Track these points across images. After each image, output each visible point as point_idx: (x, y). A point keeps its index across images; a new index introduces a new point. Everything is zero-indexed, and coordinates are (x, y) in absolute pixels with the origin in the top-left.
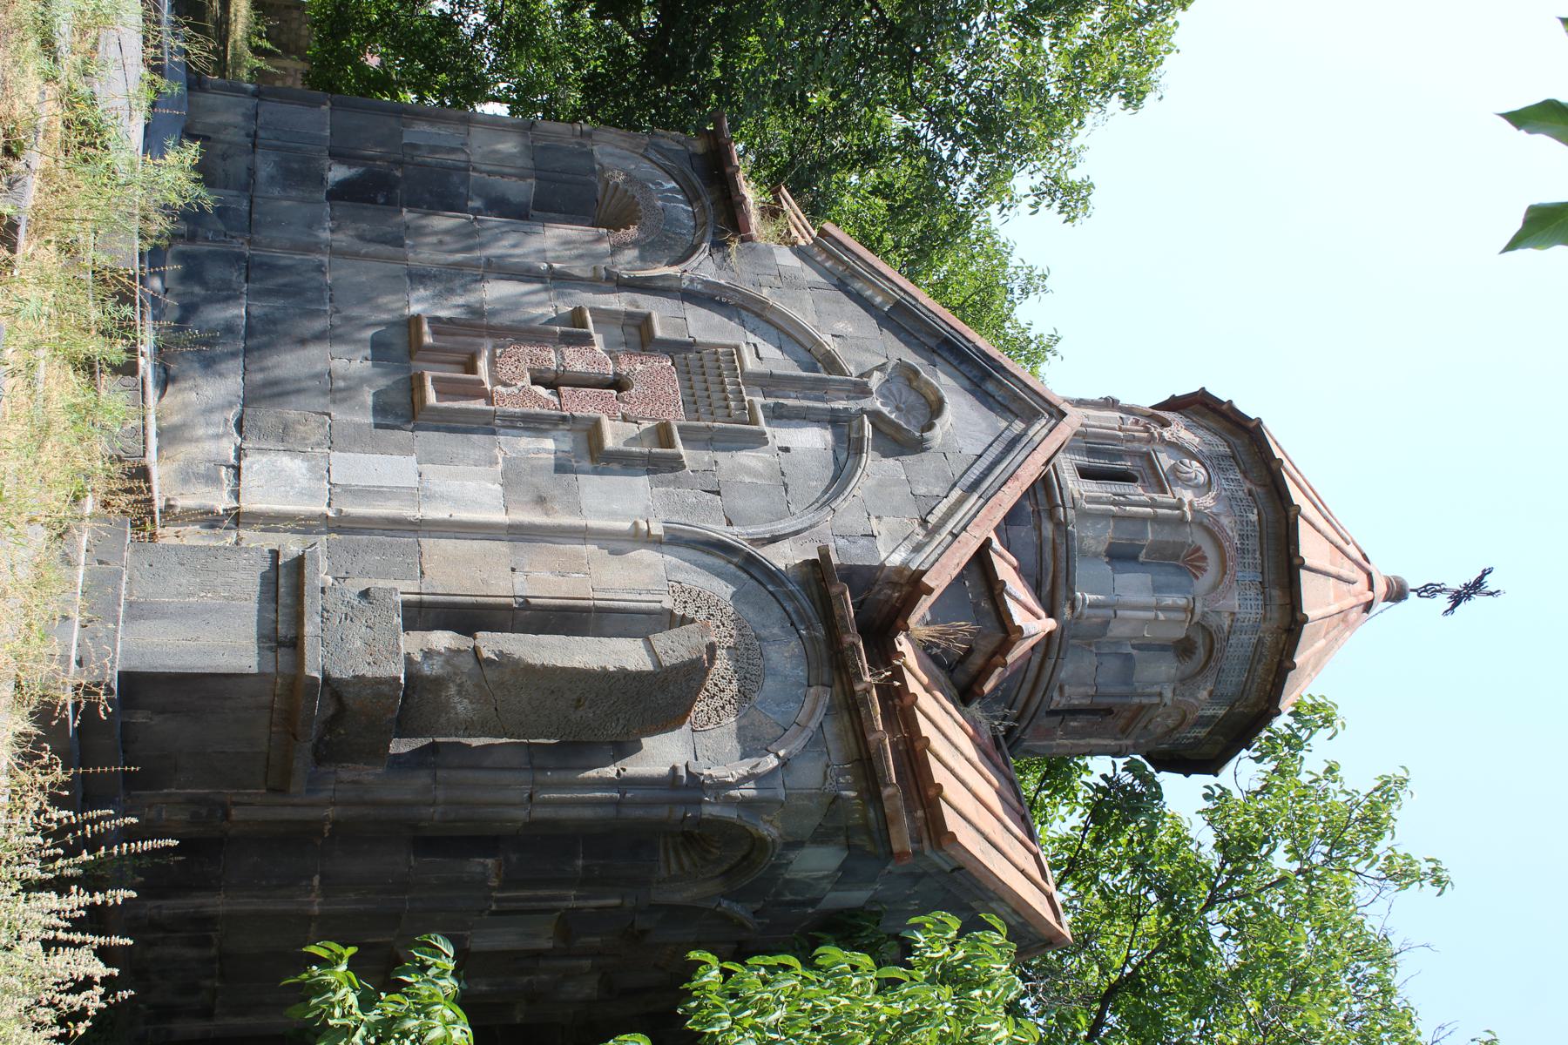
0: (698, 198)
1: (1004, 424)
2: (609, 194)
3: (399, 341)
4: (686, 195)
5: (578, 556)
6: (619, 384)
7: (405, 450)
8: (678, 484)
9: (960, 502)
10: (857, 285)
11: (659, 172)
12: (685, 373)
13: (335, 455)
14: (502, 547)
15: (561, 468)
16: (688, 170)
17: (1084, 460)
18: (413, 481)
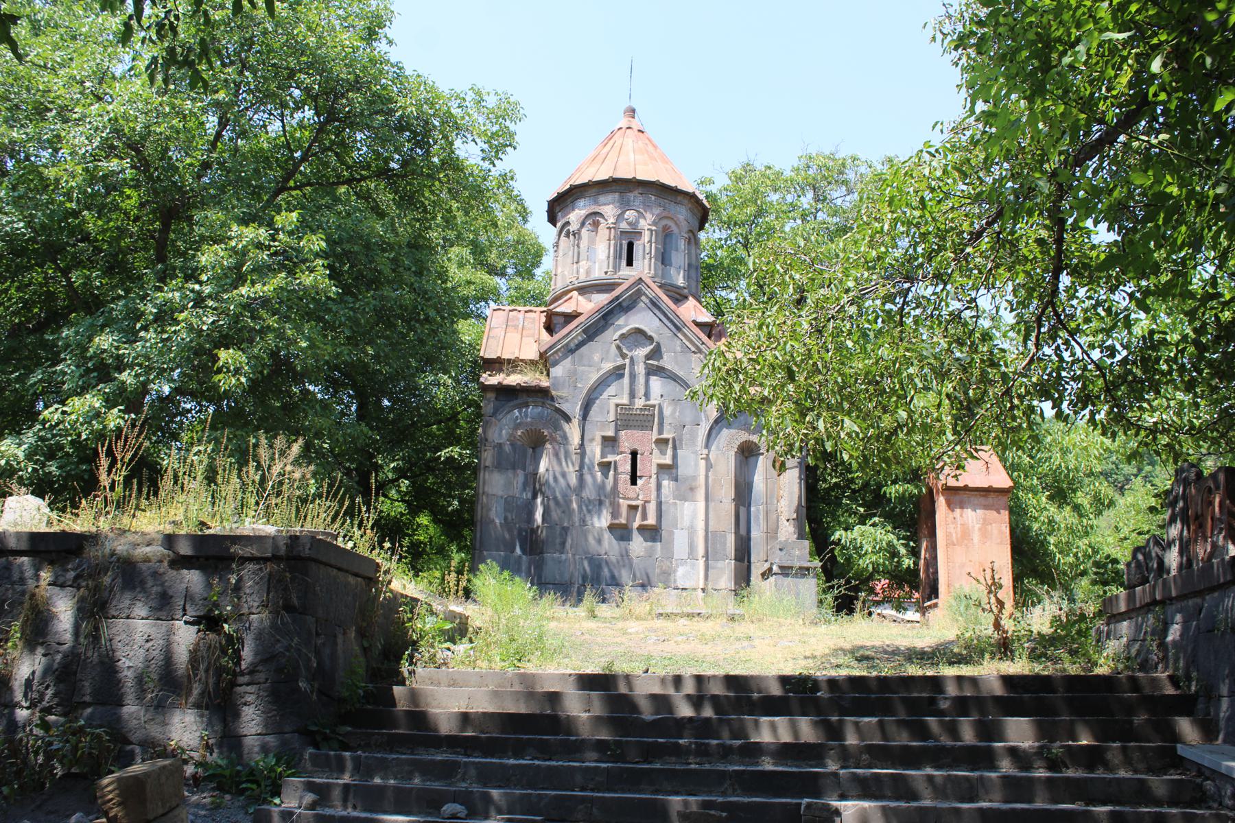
1: (642, 304)
3: (619, 532)
6: (634, 454)
7: (672, 533)
8: (681, 440)
9: (685, 335)
10: (572, 345)
12: (627, 427)
13: (675, 557)
14: (711, 505)
15: (676, 480)
16: (511, 404)
17: (624, 262)
18: (685, 533)
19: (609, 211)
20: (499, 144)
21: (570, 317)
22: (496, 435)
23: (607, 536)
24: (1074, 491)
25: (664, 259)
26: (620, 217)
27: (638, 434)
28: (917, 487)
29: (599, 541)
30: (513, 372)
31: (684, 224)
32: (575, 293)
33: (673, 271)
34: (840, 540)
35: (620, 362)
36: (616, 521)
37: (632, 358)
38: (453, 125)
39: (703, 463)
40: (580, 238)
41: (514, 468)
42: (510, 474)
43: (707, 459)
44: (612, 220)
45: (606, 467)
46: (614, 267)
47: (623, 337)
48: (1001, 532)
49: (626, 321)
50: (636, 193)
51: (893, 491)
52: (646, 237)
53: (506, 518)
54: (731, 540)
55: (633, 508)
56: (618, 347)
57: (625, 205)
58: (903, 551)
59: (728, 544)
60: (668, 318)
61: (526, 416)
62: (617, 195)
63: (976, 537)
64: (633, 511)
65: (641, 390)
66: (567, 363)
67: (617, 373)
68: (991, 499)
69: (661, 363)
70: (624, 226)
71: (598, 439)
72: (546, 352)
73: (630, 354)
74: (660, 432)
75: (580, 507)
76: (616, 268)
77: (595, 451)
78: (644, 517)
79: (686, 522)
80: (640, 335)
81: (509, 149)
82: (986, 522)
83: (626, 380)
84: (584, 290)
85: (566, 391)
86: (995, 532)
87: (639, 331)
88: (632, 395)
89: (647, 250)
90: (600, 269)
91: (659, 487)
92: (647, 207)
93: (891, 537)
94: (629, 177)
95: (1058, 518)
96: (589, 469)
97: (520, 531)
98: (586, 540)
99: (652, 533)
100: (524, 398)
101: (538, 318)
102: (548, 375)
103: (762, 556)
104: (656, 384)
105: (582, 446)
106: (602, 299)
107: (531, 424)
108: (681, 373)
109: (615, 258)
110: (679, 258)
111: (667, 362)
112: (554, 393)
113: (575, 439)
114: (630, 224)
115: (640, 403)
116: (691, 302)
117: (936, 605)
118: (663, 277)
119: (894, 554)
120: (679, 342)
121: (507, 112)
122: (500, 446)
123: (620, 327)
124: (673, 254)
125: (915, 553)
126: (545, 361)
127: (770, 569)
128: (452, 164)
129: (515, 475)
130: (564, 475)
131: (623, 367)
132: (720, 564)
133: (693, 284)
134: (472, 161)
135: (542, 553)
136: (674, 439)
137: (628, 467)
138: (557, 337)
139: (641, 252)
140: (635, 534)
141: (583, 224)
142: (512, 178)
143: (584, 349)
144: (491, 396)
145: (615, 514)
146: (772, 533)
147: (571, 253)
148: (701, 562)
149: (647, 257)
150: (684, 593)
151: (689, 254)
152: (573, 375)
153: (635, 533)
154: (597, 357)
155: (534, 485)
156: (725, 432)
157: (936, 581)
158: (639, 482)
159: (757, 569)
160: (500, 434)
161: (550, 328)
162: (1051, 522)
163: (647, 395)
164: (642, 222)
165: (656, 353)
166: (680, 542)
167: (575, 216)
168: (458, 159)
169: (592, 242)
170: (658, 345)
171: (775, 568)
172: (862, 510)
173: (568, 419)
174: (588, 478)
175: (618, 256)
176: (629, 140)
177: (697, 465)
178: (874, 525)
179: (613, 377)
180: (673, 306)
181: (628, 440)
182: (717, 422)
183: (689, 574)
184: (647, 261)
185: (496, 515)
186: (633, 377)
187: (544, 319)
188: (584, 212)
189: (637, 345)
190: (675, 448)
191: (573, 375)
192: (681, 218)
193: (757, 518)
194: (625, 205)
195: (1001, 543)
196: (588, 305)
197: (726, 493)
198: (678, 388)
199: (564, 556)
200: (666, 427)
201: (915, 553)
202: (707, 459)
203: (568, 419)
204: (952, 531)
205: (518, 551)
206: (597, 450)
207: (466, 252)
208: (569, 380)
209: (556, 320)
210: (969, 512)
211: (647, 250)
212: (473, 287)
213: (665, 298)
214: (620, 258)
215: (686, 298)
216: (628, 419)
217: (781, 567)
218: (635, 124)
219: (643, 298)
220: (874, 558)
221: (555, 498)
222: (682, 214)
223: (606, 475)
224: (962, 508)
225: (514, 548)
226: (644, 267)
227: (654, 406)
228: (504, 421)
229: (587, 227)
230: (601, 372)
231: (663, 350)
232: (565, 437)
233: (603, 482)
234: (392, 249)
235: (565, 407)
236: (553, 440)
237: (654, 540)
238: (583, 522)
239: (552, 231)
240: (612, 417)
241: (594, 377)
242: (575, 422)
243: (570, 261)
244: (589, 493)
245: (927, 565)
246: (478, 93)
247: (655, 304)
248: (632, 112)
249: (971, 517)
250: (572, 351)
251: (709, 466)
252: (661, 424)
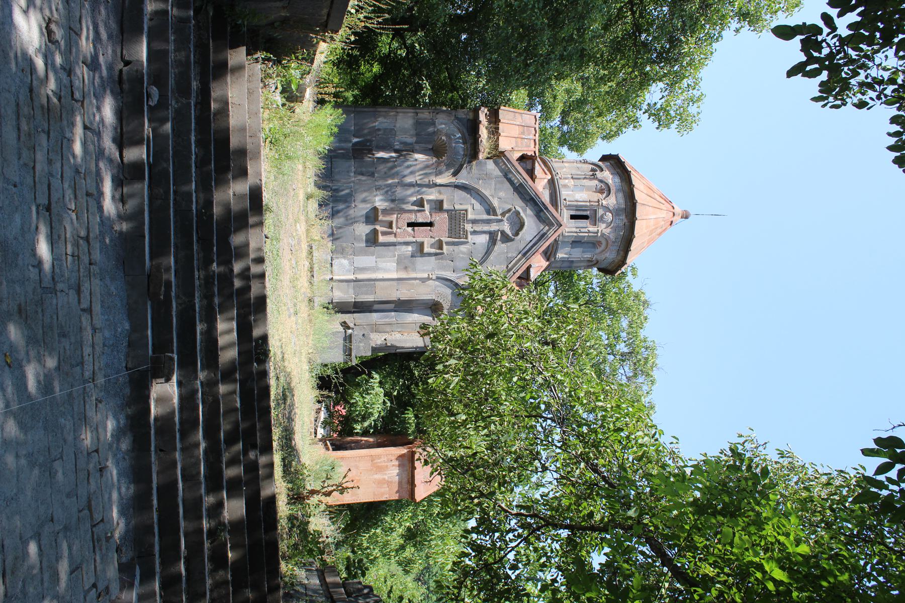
1: (542, 227)
3: (372, 215)
5: (413, 284)
6: (430, 224)
7: (373, 254)
8: (442, 259)
9: (520, 260)
10: (510, 176)
11: (456, 130)
12: (450, 218)
14: (394, 283)
15: (412, 256)
16: (465, 131)
17: (573, 213)
18: (374, 264)
19: (612, 201)
20: (661, 116)
21: (531, 173)
22: (441, 121)
23: (369, 206)
24: (414, 546)
25: (577, 242)
26: (607, 209)
27: (446, 226)
28: (413, 432)
29: (364, 201)
30: (489, 132)
31: (603, 257)
32: (549, 177)
33: (567, 249)
34: (372, 378)
35: (499, 212)
36: (380, 213)
37: (502, 220)
38: (674, 81)
39: (426, 276)
40: (591, 179)
41: (417, 135)
42: (413, 132)
43: (429, 279)
44: (604, 203)
45: (420, 203)
46: (569, 206)
47: (518, 213)
48: (383, 494)
49: (529, 216)
50: (625, 221)
51: (410, 415)
52: (592, 229)
53: (379, 130)
54: (370, 298)
55: (390, 225)
56: (509, 210)
57: (616, 212)
58: (366, 424)
59: (366, 297)
60: (532, 247)
61: (457, 143)
62: (623, 206)
63: (378, 476)
64: (387, 225)
65: (478, 228)
66: (497, 172)
67: (490, 210)
68: (406, 487)
69: (499, 243)
70: (601, 212)
71: (440, 197)
72: (505, 156)
73: (505, 219)
74: (448, 243)
75: (390, 185)
76: (569, 207)
77: (432, 195)
78: (384, 234)
79: (382, 265)
80: (519, 226)
81: (657, 124)
82: (389, 483)
83: (485, 217)
84: (552, 183)
85: (476, 172)
86: (383, 490)
87: (522, 225)
88: (474, 222)
89: (583, 230)
90: (568, 195)
91: (407, 244)
92: (615, 229)
93: (376, 415)
94: (637, 215)
95: (394, 534)
96: (418, 191)
97: (371, 141)
98: (365, 191)
99: (372, 240)
100: (470, 141)
101: (531, 149)
102: (488, 158)
103: (358, 322)
104: (483, 239)
105: (435, 185)
106: (545, 197)
107: (450, 147)
108: (492, 257)
109: (576, 206)
110: (577, 254)
111: (500, 247)
112: (474, 163)
113: (440, 180)
114: (602, 216)
115: (469, 227)
116: (545, 264)
117: (328, 449)
118: (563, 242)
119: (364, 418)
120: (515, 255)
121: (685, 122)
122: (434, 124)
123: (525, 211)
124: (580, 250)
125: (365, 433)
126: (498, 155)
127: (349, 328)
128: (645, 81)
129: (412, 136)
130: (412, 173)
131: (495, 214)
132: (351, 291)
133: (558, 265)
134: (647, 96)
135: (354, 158)
136: (443, 254)
137: (420, 220)
138: (516, 164)
139: (581, 225)
140: (371, 227)
141: (601, 181)
142: (635, 127)
143: (508, 185)
144: (471, 116)
145: (386, 212)
146: (376, 328)
147: (580, 173)
148: (352, 277)
149: (578, 230)
150: (329, 265)
151: (581, 261)
152: (487, 177)
153: (371, 227)
154: (502, 194)
155: (405, 151)
156: (449, 291)
157: (346, 449)
158: (410, 229)
159: (348, 318)
160: (442, 124)
161: (523, 158)
162: (392, 530)
163: (475, 233)
164: (604, 226)
165: (506, 239)
166: (366, 261)
167: (607, 175)
168: (649, 85)
169: (588, 189)
170: (512, 240)
171: (350, 331)
172: (395, 393)
173: (455, 174)
174: (410, 191)
175: (578, 208)
176: (664, 214)
177: (424, 271)
178: (384, 402)
179: (487, 207)
180: (541, 250)
181: (441, 220)
182: (456, 285)
183: (343, 269)
184: (574, 230)
185: (381, 122)
186: (488, 222)
187: (529, 154)
188: (610, 182)
189: (512, 224)
190: (436, 254)
191: (487, 177)
192: (607, 255)
193: (386, 317)
194: (616, 212)
195: (374, 495)
196: (540, 186)
197: (404, 293)
198: (481, 256)
199: (352, 174)
200: (451, 248)
201: (365, 433)
202: (429, 279)
203: (455, 174)
204: (382, 460)
205: (355, 140)
206: (432, 197)
207: (577, 95)
208: (484, 174)
209: (529, 163)
210: (396, 471)
211: (583, 230)
212: (551, 100)
213: (547, 244)
214: (577, 210)
215: (548, 260)
216: (456, 219)
217: (351, 335)
218: (677, 219)
219: (547, 228)
220: (360, 403)
221: (395, 167)
222: (610, 255)
223: (414, 204)
224: (399, 466)
225: (357, 137)
226: (570, 228)
227: (466, 238)
228: (452, 126)
229: (599, 185)
230: (490, 198)
231: (509, 244)
233: (407, 203)
234: (580, 37)
235: (464, 172)
237: (367, 241)
238: (378, 188)
239: (596, 159)
240: (457, 207)
241: (487, 193)
242: (453, 180)
243: (574, 172)
244: (400, 192)
245: (357, 442)
246: (699, 99)
247: (542, 236)
248: (686, 216)
249: (393, 473)
250: (506, 176)
251: (423, 280)
252: (454, 244)
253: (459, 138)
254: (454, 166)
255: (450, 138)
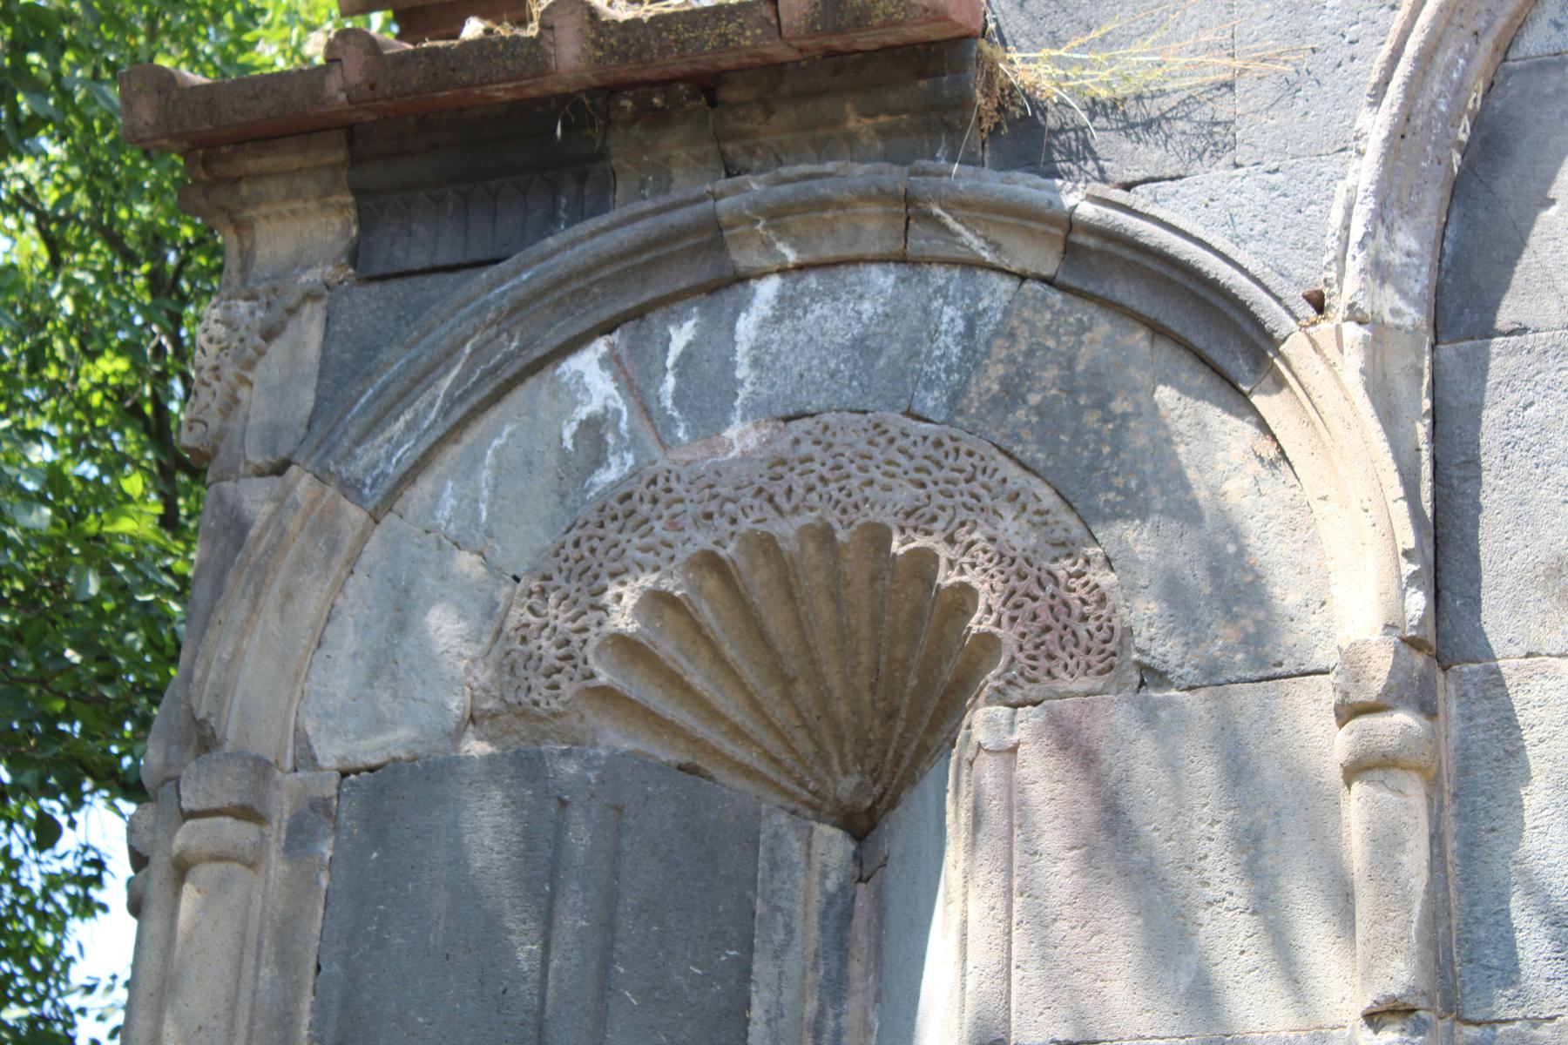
0: (712, 236)
2: (654, 697)
4: (670, 302)
11: (501, 433)
22: (338, 677)
61: (708, 394)
105: (1446, 640)
112: (1031, 68)
113: (1346, 579)
122: (391, 797)
173: (1224, 340)
228: (442, 497)
232: (1230, 589)
235: (1198, 213)
236: (1072, 640)
242: (1328, 369)
253: (634, 380)
254: (1094, 388)
255: (624, 506)
